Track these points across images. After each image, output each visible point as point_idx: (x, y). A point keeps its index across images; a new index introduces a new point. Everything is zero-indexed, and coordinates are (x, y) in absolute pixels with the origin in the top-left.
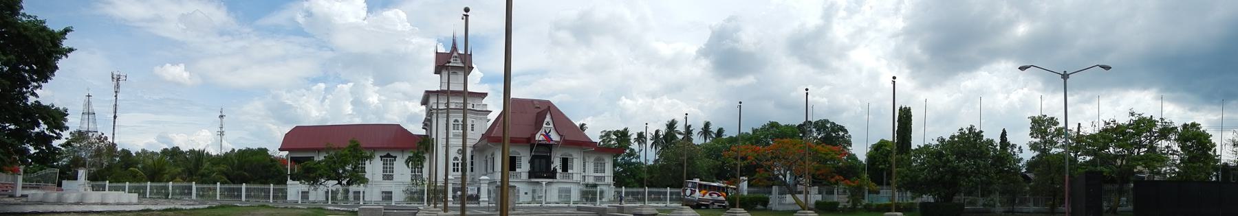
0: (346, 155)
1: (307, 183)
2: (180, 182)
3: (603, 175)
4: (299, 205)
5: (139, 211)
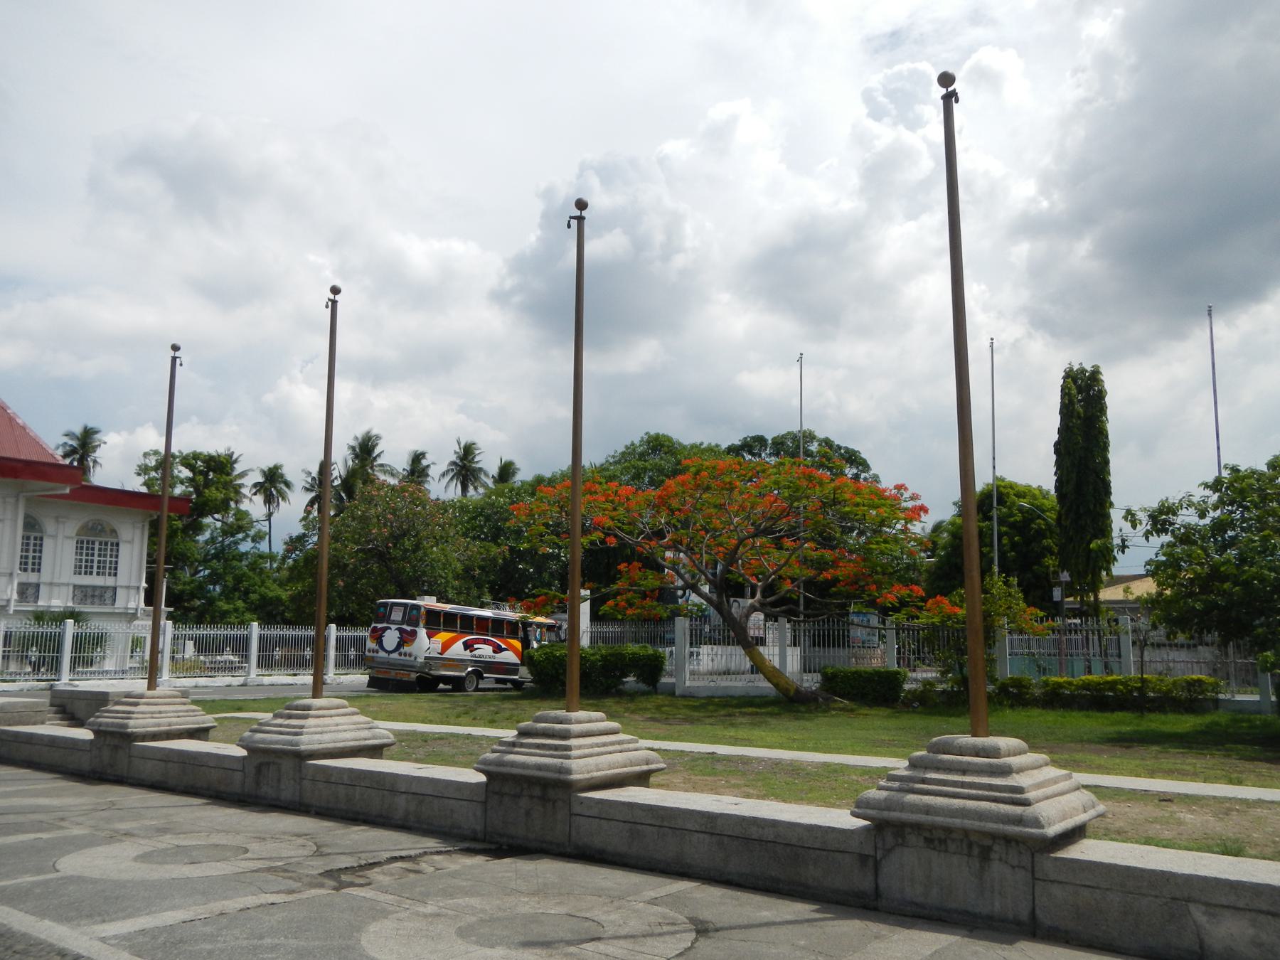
3: (109, 581)
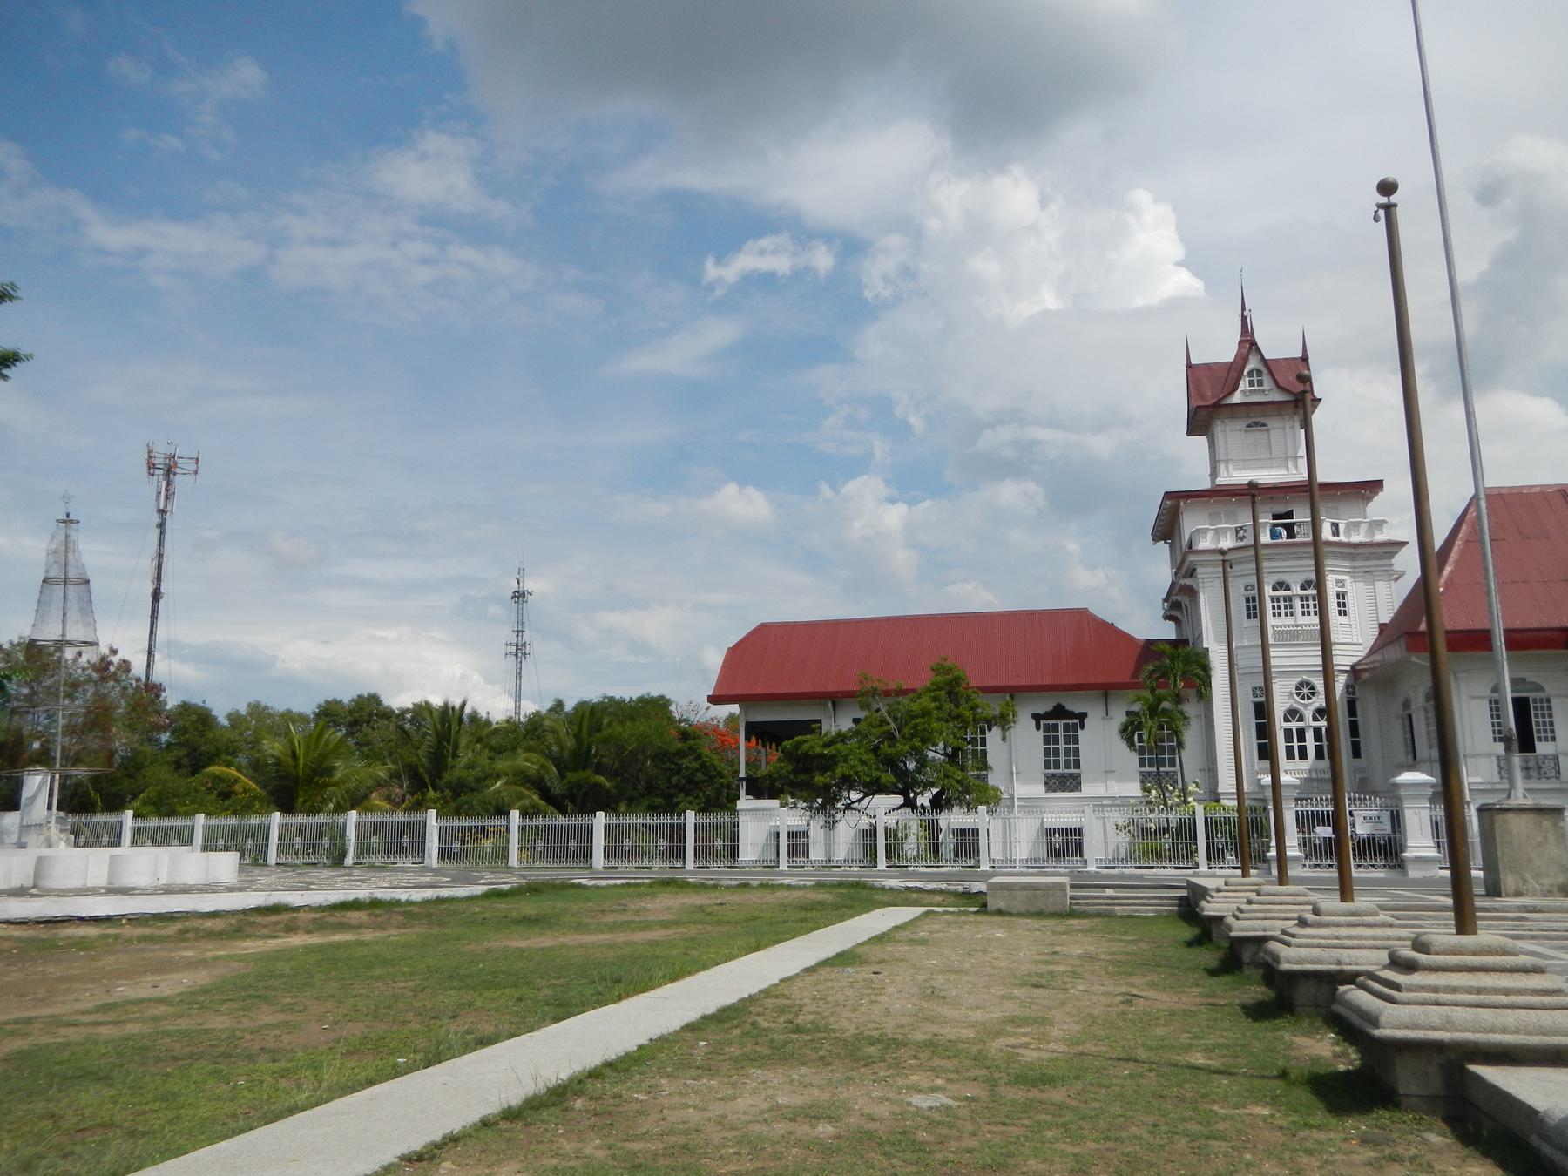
0: (925, 713)
1: (802, 805)
2: (380, 809)
4: (782, 874)
5: (244, 912)
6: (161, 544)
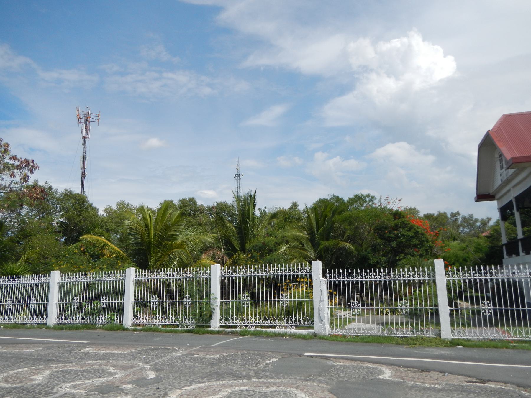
6: (84, 152)
